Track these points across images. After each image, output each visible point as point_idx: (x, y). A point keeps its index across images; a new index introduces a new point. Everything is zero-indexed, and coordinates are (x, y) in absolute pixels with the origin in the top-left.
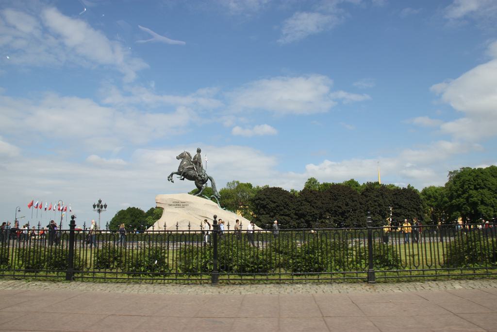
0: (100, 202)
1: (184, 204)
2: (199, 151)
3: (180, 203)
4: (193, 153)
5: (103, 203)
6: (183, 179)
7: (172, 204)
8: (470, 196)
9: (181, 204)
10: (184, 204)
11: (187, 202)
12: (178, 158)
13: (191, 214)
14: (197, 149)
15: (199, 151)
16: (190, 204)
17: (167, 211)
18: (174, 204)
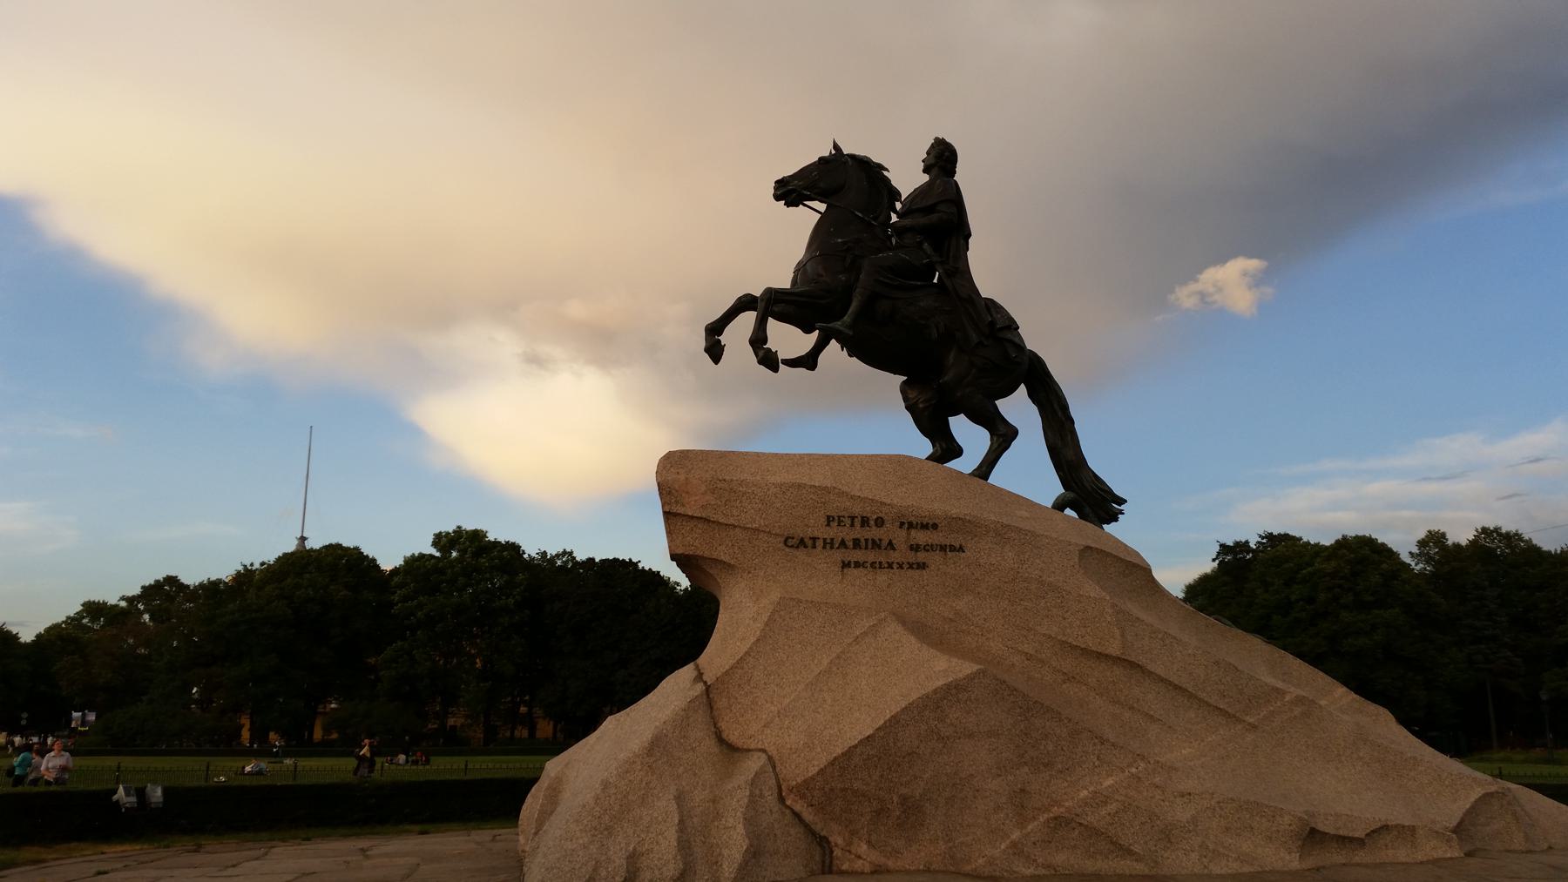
1: (921, 537)
2: (942, 158)
6: (808, 361)
9: (900, 536)
10: (921, 537)
12: (790, 191)
15: (942, 158)
18: (834, 532)
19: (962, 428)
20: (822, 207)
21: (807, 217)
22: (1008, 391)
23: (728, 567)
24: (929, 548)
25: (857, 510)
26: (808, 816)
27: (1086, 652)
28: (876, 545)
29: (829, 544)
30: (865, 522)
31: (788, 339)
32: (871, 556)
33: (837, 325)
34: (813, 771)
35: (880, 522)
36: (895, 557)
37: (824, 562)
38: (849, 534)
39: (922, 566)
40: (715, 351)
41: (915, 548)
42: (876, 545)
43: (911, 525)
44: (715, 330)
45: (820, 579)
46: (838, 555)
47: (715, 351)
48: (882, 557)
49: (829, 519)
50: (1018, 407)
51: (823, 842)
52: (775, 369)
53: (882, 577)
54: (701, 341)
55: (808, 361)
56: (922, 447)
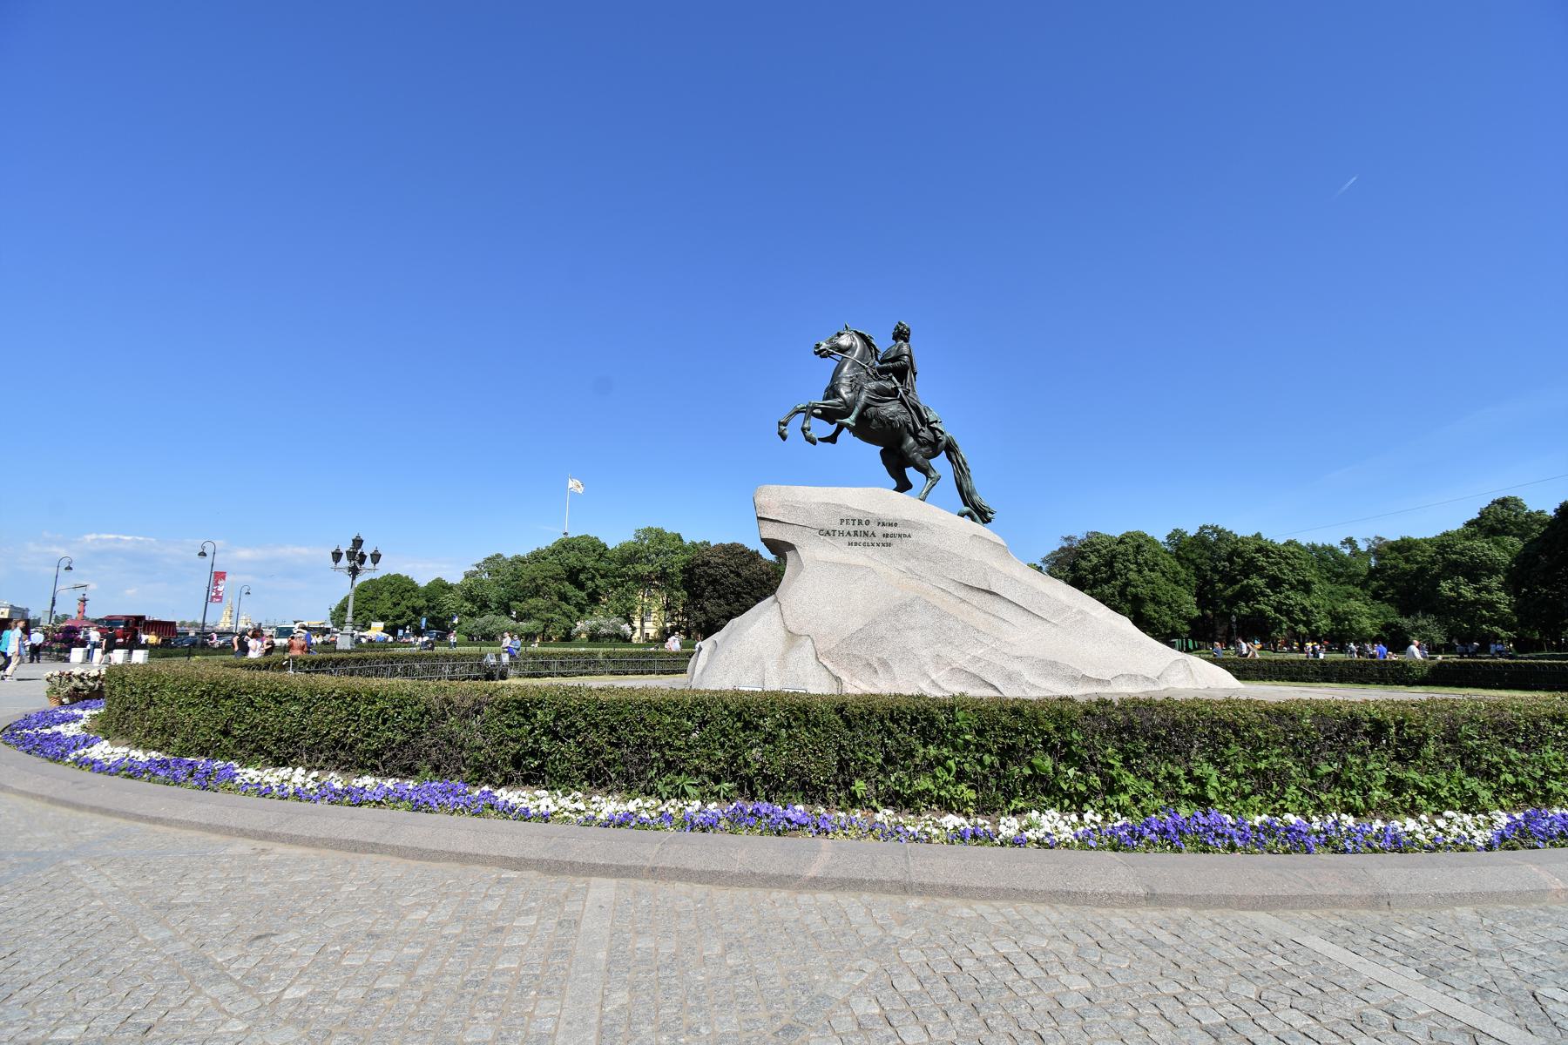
0: (358, 542)
1: (890, 530)
2: (901, 334)
3: (872, 527)
4: (884, 343)
5: (367, 549)
6: (832, 439)
8: (1127, 584)
9: (879, 530)
10: (890, 530)
11: (907, 523)
13: (921, 578)
15: (901, 334)
16: (914, 533)
17: (812, 555)
18: (845, 528)
19: (911, 473)
22: (936, 454)
23: (791, 547)
24: (893, 536)
25: (856, 516)
26: (830, 666)
27: (972, 587)
28: (866, 534)
30: (860, 522)
31: (823, 428)
32: (863, 540)
33: (847, 421)
35: (868, 523)
36: (875, 540)
38: (852, 529)
41: (886, 536)
42: (866, 534)
46: (847, 539)
47: (784, 438)
48: (868, 540)
50: (940, 463)
51: (837, 679)
52: (814, 443)
53: (869, 551)
55: (832, 439)
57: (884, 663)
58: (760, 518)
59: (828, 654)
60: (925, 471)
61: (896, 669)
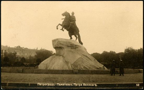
1: (76, 46)
3: (74, 46)
7: (70, 46)
10: (76, 46)
11: (78, 46)
12: (63, 15)
14: (72, 12)
15: (73, 13)
18: (71, 46)
19: (73, 36)
20: (65, 16)
21: (64, 17)
23: (63, 48)
25: (72, 44)
28: (73, 47)
29: (70, 47)
32: (73, 48)
34: (73, 63)
37: (70, 48)
39: (75, 49)
40: (57, 29)
42: (73, 47)
43: (75, 46)
44: (57, 27)
45: (70, 49)
46: (71, 48)
47: (57, 29)
49: (71, 45)
54: (56, 27)
56: (70, 38)
57: (77, 65)
58: (60, 43)
59: (72, 64)
60: (76, 36)
61: (78, 66)
